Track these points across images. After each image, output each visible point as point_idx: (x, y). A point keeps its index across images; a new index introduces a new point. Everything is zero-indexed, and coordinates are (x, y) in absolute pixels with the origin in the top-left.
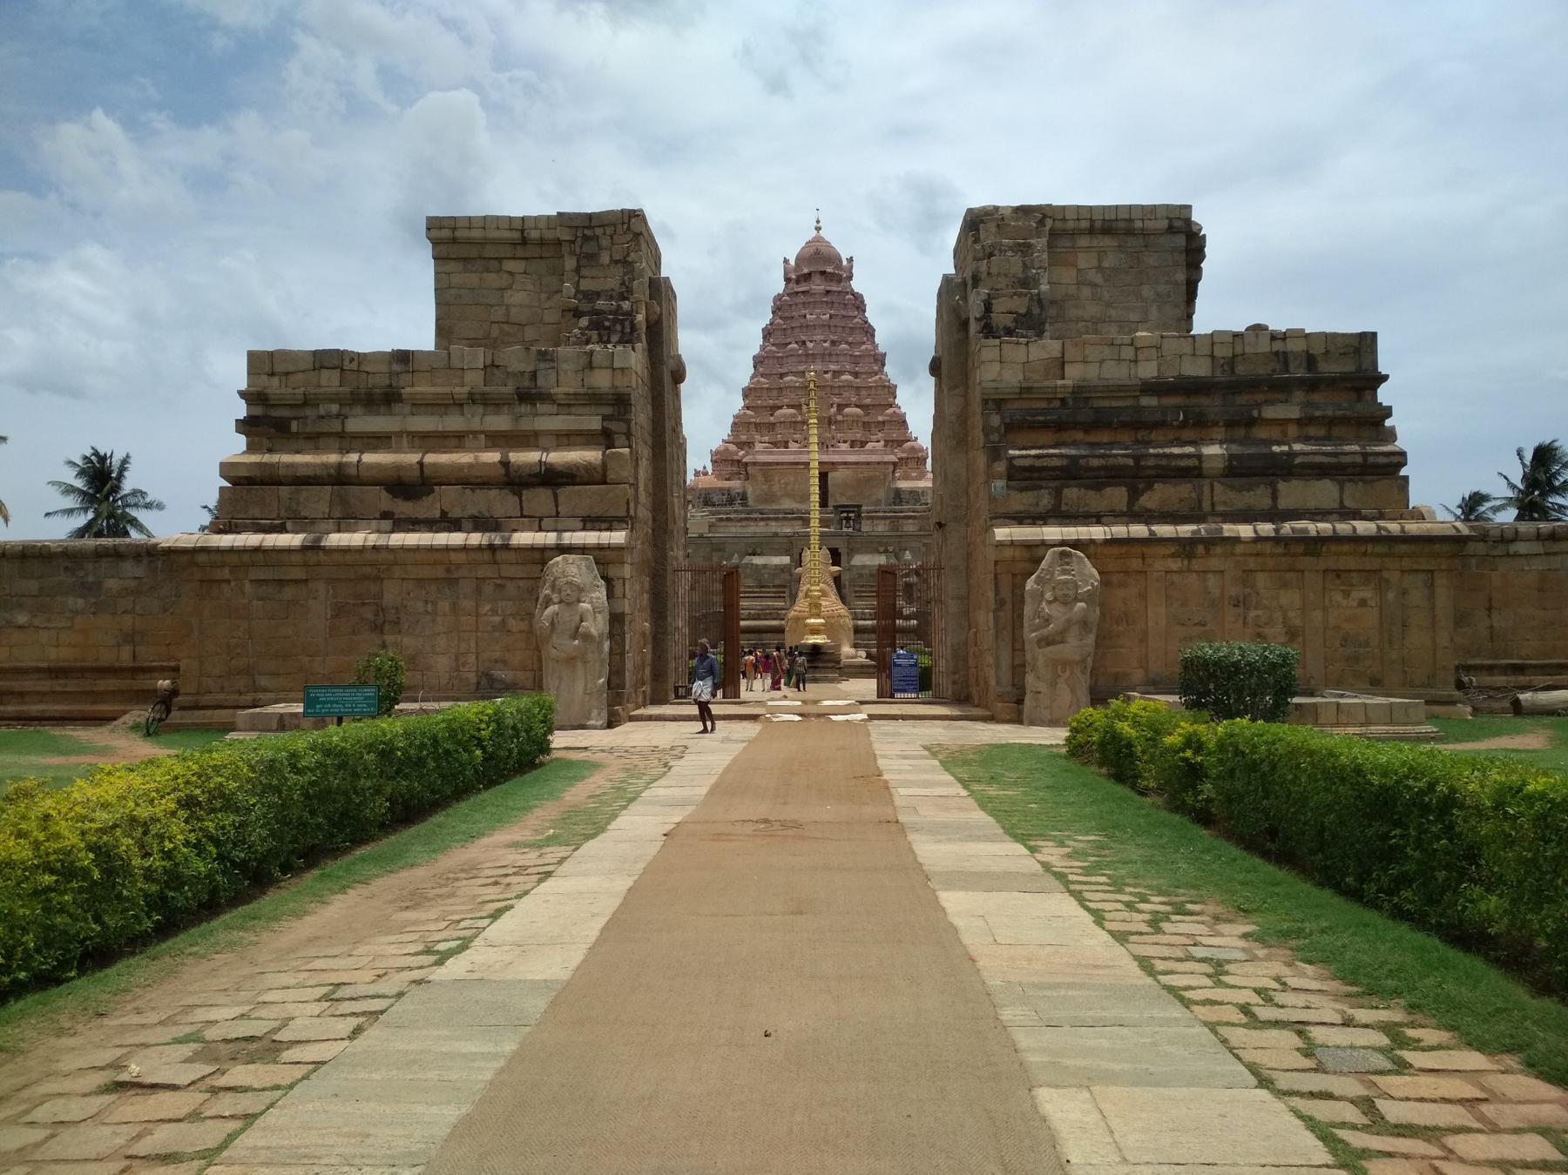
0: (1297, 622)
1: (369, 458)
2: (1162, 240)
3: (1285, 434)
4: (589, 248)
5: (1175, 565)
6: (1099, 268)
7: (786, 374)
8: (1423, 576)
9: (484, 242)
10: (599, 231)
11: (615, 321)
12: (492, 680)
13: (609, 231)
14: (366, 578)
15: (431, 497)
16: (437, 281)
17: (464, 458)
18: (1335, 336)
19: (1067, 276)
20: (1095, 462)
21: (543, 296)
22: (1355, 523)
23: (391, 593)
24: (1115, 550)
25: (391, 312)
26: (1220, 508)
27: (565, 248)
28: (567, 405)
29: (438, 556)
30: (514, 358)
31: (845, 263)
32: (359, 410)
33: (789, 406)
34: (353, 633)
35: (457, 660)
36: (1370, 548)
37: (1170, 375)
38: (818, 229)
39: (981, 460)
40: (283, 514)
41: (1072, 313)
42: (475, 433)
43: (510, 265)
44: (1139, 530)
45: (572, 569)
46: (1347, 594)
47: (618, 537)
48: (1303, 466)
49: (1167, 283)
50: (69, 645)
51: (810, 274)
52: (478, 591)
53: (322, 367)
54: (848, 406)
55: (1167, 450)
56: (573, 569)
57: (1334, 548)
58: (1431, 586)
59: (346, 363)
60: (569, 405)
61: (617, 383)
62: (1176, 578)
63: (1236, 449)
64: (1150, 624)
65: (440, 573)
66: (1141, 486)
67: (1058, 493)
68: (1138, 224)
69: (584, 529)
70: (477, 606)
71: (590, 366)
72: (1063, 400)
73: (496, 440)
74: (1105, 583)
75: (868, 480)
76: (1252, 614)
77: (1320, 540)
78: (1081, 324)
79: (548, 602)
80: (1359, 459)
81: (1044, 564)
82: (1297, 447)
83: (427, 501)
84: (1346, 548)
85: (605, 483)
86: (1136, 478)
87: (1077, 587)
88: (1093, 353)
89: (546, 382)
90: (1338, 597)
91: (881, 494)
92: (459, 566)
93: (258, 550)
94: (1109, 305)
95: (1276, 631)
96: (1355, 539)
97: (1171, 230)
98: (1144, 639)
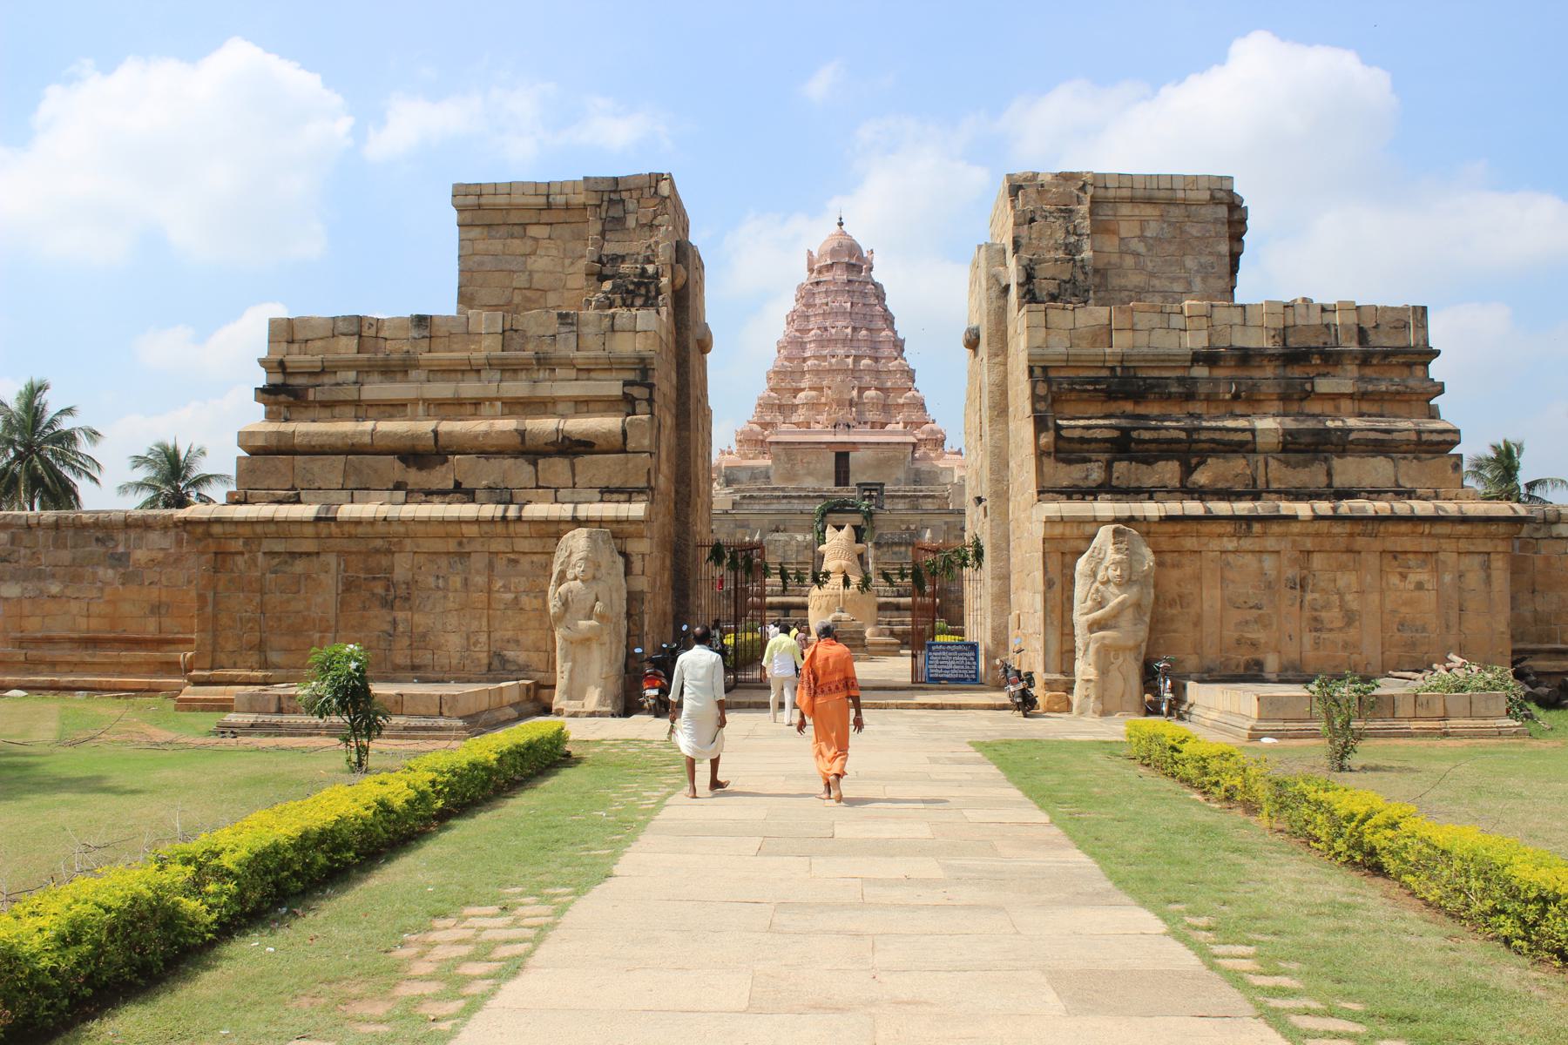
0: (1355, 606)
1: (385, 426)
2: (1203, 211)
3: (1337, 408)
4: (616, 212)
5: (1231, 544)
6: (1142, 238)
8: (1477, 560)
9: (508, 209)
10: (625, 195)
11: (638, 285)
12: (504, 661)
13: (635, 194)
14: (377, 551)
15: (444, 469)
16: (461, 248)
17: (477, 426)
18: (1385, 309)
19: (1110, 244)
20: (1146, 435)
21: (567, 262)
23: (402, 567)
24: (1169, 528)
26: (1274, 486)
28: (585, 371)
29: (450, 529)
32: (376, 377)
34: (364, 608)
35: (468, 638)
36: (1427, 528)
37: (1221, 343)
38: (841, 224)
39: (1028, 430)
40: (298, 484)
41: (1115, 281)
42: (492, 400)
43: (533, 231)
44: (1194, 507)
46: (1404, 577)
47: (637, 509)
48: (1357, 442)
50: (99, 616)
52: (491, 566)
55: (1220, 424)
57: (1391, 528)
58: (1487, 567)
59: (365, 328)
60: (589, 370)
61: (638, 347)
62: (1231, 557)
63: (1290, 423)
64: (1206, 606)
65: (452, 546)
66: (1194, 461)
67: (1109, 467)
68: (1180, 194)
69: (601, 501)
70: (490, 582)
71: (613, 329)
72: (1113, 369)
73: (514, 406)
74: (1160, 564)
75: (889, 459)
76: (1309, 597)
77: (1378, 519)
79: (562, 578)
80: (1414, 437)
82: (1352, 422)
83: (440, 471)
84: (1404, 528)
85: (624, 451)
86: (1189, 452)
88: (1142, 320)
89: (565, 348)
90: (1395, 580)
91: (901, 474)
92: (471, 538)
93: (271, 521)
94: (1152, 275)
95: (1332, 616)
97: (1214, 200)
98: (1197, 623)
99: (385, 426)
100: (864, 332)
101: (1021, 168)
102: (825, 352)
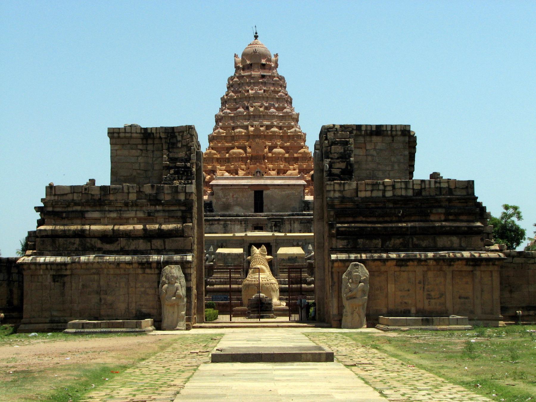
1: (93, 227)
3: (440, 218)
6: (375, 149)
7: (237, 127)
11: (184, 172)
18: (459, 181)
22: (463, 252)
25: (97, 169)
27: (163, 141)
30: (147, 189)
31: (273, 58)
32: (88, 208)
33: (238, 148)
35: (128, 305)
38: (256, 37)
45: (175, 271)
49: (401, 155)
51: (251, 65)
53: (74, 192)
54: (276, 147)
56: (174, 271)
58: (492, 276)
64: (389, 290)
76: (426, 287)
78: (368, 171)
79: (164, 283)
81: (349, 269)
83: (115, 245)
85: (183, 236)
87: (361, 277)
96: (462, 259)
98: (387, 296)
99: (93, 227)
100: (272, 110)
101: (329, 123)
102: (246, 123)
